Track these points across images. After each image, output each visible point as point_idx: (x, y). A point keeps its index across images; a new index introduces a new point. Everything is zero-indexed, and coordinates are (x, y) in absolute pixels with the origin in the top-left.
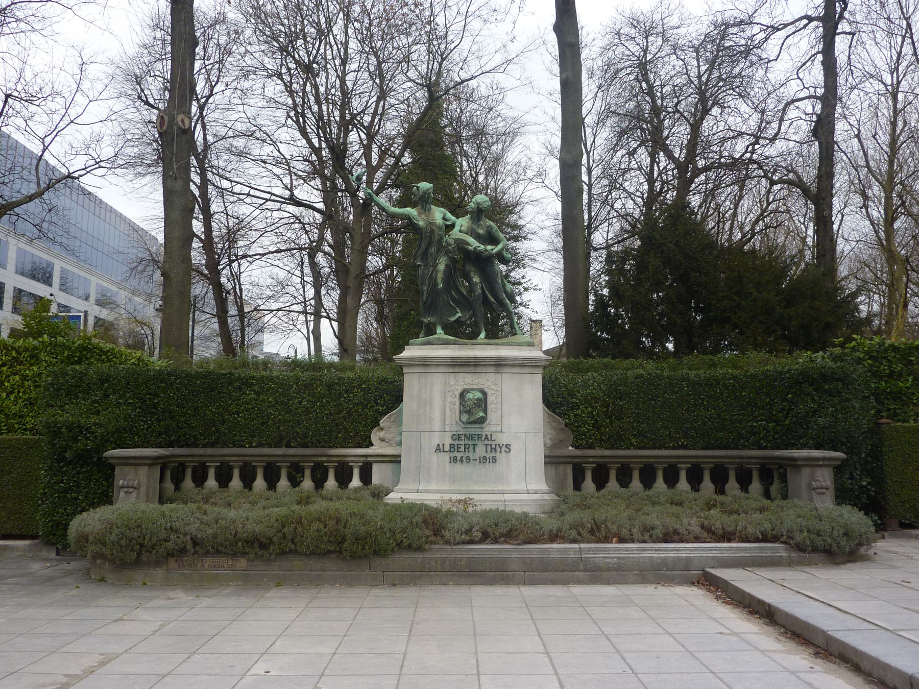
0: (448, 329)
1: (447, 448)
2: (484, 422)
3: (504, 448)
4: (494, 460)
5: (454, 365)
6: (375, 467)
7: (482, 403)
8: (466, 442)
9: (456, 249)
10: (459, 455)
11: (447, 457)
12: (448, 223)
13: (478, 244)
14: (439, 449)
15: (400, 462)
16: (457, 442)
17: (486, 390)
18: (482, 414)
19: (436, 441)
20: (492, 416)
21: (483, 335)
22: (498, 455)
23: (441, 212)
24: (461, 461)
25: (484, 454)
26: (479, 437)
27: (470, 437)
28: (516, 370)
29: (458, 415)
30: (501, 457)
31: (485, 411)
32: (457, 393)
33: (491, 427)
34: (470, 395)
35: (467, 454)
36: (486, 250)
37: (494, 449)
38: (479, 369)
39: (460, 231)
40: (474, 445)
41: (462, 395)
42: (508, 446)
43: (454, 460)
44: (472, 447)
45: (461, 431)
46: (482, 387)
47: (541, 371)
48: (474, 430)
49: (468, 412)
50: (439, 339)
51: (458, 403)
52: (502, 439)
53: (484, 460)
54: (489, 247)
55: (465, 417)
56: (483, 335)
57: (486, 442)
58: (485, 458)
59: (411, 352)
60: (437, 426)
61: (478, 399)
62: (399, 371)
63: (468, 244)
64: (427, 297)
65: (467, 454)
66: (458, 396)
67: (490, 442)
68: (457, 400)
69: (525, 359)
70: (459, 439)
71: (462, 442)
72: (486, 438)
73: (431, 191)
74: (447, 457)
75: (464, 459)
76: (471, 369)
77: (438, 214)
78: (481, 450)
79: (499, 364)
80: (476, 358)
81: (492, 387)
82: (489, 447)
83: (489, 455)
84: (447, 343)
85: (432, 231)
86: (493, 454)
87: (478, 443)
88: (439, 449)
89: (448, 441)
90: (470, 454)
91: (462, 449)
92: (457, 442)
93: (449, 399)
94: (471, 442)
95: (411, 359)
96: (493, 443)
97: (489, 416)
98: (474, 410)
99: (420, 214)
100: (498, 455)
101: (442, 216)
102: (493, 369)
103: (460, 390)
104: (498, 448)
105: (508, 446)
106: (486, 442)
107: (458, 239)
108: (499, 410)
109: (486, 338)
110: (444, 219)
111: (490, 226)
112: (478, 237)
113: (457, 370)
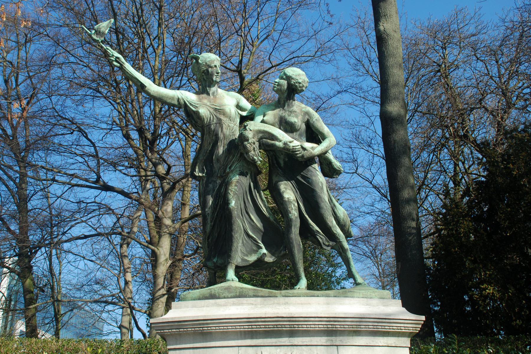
5: (252, 334)
12: (244, 114)
13: (291, 139)
21: (303, 282)
23: (233, 96)
47: (407, 342)
50: (228, 289)
54: (308, 145)
56: (303, 282)
64: (213, 227)
73: (218, 64)
77: (229, 100)
80: (291, 319)
84: (241, 295)
95: (179, 324)
99: (200, 100)
101: (234, 103)
107: (260, 132)
109: (310, 287)
110: (238, 107)
111: (307, 113)
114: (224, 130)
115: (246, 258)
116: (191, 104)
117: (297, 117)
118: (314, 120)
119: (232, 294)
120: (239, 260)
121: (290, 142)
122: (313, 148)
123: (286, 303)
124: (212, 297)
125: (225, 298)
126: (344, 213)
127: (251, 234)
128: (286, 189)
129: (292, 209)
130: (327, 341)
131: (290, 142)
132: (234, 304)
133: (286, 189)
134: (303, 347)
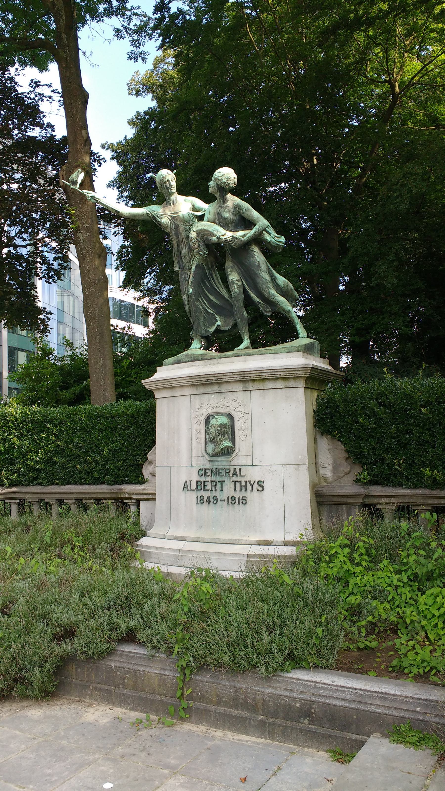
0: (209, 342)
1: (194, 486)
2: (232, 453)
3: (256, 486)
4: (244, 501)
6: (142, 504)
7: (228, 430)
8: (213, 479)
9: (201, 243)
10: (206, 494)
11: (193, 496)
14: (186, 487)
15: (154, 500)
16: (203, 479)
17: (233, 413)
18: (227, 443)
19: (184, 478)
20: (241, 445)
22: (248, 494)
24: (208, 502)
25: (232, 494)
26: (227, 471)
27: (217, 472)
28: (270, 385)
29: (203, 445)
30: (253, 497)
31: (233, 440)
32: (202, 419)
33: (239, 460)
34: (213, 422)
35: (214, 494)
36: (236, 238)
37: (243, 487)
38: (225, 388)
39: (208, 221)
40: (222, 482)
41: (207, 421)
42: (260, 484)
43: (200, 500)
44: (219, 485)
45: (208, 465)
46: (227, 410)
48: (221, 463)
49: (213, 441)
51: (203, 432)
52: (253, 475)
53: (232, 501)
55: (211, 448)
56: (246, 342)
57: (235, 478)
58: (233, 498)
59: (163, 373)
60: (184, 460)
61: (221, 426)
62: (150, 395)
63: (212, 234)
65: (214, 494)
66: (203, 422)
67: (239, 479)
68: (202, 427)
69: (261, 371)
70: (205, 475)
71: (209, 479)
72: (235, 473)
74: (193, 496)
75: (211, 499)
76: (216, 388)
78: (229, 489)
79: (247, 380)
80: (215, 375)
81: (239, 409)
82: (238, 485)
83: (238, 495)
85: (177, 228)
86: (243, 494)
87: (226, 479)
88: (186, 487)
89: (195, 478)
90: (218, 494)
91: (209, 487)
92: (203, 479)
93: (195, 427)
94: (219, 479)
96: (243, 480)
97: (236, 445)
98: (221, 437)
100: (248, 494)
102: (239, 386)
103: (205, 415)
104: (249, 487)
105: (260, 484)
106: (235, 478)
108: (249, 438)
112: (225, 224)
113: (201, 390)
114: (182, 233)
115: (208, 329)
116: (157, 216)
117: (229, 211)
118: (244, 210)
119: (189, 359)
120: (203, 332)
121: (223, 235)
122: (244, 236)
123: (218, 363)
124: (179, 362)
125: (185, 362)
126: (284, 282)
127: (210, 311)
128: (231, 272)
129: (235, 288)
130: (243, 387)
131: (223, 235)
132: (188, 367)
133: (231, 272)
134: (228, 393)
